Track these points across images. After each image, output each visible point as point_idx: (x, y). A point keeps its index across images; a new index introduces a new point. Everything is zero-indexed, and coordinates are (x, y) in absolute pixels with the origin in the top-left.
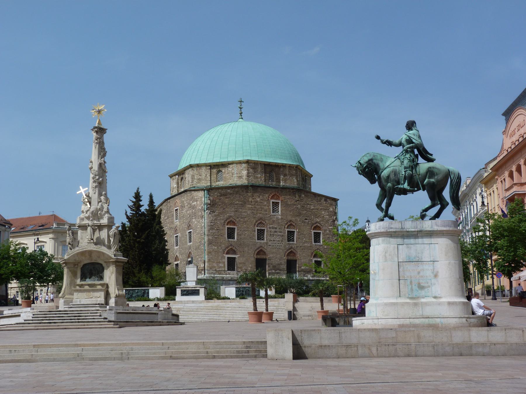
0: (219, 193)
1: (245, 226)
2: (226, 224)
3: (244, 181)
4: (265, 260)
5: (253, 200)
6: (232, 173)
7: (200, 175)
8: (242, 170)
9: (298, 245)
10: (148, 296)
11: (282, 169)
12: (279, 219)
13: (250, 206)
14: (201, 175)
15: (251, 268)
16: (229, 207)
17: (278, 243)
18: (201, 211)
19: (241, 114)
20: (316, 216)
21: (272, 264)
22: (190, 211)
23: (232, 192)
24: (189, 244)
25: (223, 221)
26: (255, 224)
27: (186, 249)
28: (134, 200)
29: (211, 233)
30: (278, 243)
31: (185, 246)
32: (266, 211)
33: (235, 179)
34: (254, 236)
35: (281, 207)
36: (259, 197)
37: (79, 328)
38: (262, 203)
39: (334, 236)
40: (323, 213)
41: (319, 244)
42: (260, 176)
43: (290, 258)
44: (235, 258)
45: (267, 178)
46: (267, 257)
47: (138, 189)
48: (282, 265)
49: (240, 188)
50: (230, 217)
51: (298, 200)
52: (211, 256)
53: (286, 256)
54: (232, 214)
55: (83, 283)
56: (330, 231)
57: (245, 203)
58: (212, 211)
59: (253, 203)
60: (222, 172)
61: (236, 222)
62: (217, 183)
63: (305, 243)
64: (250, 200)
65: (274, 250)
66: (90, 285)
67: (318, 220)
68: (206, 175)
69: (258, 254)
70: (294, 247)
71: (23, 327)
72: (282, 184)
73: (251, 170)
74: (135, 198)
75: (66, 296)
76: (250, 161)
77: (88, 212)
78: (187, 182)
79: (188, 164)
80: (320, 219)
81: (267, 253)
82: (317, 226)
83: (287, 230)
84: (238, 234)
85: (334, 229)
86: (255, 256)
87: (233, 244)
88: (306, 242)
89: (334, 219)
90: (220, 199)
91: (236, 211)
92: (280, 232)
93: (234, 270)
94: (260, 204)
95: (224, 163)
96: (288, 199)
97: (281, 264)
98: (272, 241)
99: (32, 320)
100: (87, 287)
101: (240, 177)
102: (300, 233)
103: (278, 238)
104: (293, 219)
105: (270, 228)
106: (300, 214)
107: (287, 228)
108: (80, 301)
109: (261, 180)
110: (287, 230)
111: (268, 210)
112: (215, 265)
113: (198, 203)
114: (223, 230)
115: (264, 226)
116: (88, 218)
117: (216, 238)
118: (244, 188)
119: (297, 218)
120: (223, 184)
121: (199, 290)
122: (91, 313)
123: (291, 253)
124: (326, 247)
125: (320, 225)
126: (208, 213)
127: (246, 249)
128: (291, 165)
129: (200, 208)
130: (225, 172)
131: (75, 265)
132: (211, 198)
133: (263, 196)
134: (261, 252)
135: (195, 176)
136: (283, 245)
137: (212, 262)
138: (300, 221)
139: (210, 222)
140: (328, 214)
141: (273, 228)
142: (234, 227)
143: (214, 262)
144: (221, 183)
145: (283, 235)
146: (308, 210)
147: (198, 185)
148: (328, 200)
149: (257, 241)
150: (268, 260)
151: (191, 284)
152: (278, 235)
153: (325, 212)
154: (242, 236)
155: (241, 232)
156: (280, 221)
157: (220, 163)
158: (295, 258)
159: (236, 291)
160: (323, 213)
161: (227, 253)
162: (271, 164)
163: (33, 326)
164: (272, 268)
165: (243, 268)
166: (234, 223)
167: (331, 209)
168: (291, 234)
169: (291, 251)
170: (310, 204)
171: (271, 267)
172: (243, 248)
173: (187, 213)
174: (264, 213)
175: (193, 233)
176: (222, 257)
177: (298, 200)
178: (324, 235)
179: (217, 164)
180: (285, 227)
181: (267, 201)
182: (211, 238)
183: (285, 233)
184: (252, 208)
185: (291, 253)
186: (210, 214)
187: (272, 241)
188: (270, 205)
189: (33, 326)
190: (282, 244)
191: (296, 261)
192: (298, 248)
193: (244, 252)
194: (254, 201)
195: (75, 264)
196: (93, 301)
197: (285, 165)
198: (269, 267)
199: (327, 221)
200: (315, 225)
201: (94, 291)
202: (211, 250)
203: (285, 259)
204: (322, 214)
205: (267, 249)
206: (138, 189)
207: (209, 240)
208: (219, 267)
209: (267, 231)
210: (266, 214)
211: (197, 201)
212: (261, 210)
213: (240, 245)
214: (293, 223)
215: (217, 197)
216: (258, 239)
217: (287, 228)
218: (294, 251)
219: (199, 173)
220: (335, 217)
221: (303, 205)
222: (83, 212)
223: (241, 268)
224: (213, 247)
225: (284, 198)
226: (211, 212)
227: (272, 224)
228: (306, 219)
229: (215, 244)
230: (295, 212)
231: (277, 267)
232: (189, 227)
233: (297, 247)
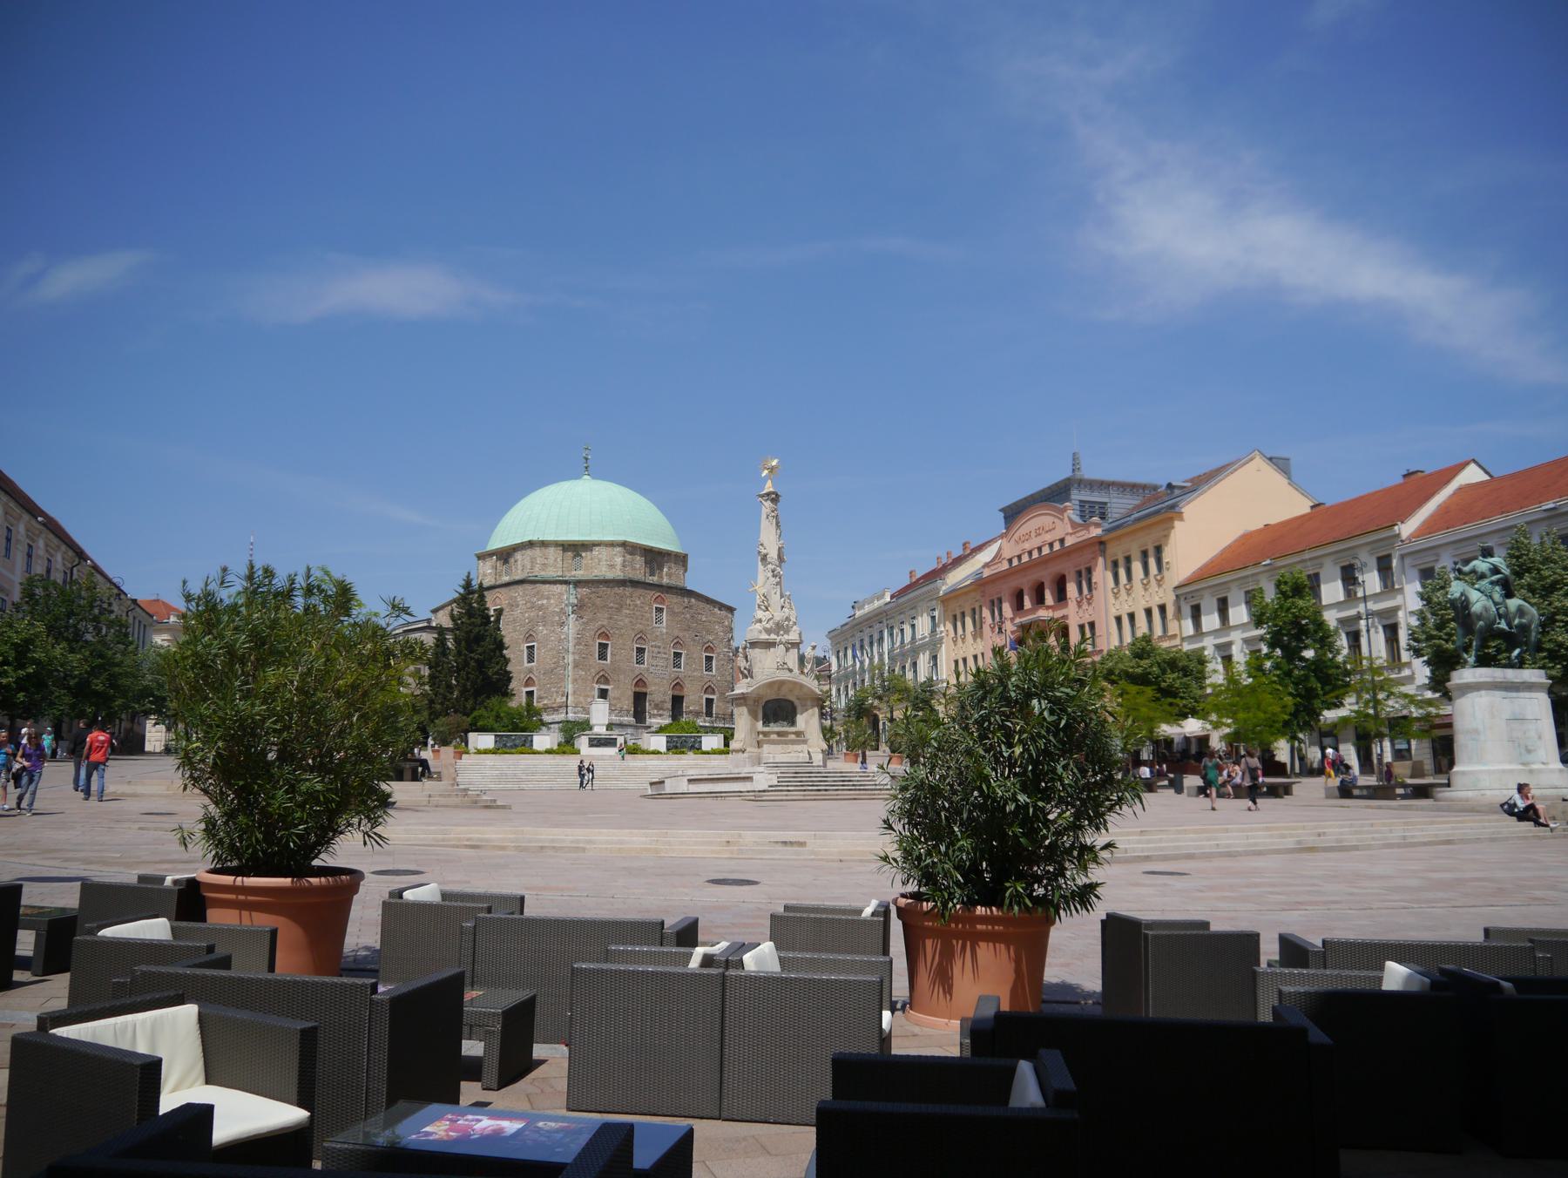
3: (617, 574)
4: (645, 694)
8: (615, 555)
10: (532, 745)
11: (666, 558)
13: (628, 612)
16: (600, 611)
18: (559, 616)
19: (586, 468)
20: (709, 632)
22: (532, 614)
24: (526, 665)
25: (593, 633)
27: (520, 672)
28: (462, 591)
31: (518, 668)
33: (604, 569)
34: (632, 657)
37: (855, 799)
38: (642, 607)
40: (717, 627)
41: (711, 673)
43: (677, 693)
47: (469, 573)
50: (603, 626)
54: (605, 623)
55: (766, 729)
57: (622, 607)
59: (632, 608)
60: (581, 556)
62: (573, 573)
63: (694, 671)
64: (628, 602)
66: (779, 734)
68: (556, 559)
71: (787, 795)
72: (665, 581)
74: (463, 588)
75: (748, 750)
77: (771, 622)
78: (520, 567)
79: (526, 539)
83: (673, 651)
86: (633, 688)
87: (606, 668)
88: (695, 670)
92: (665, 653)
99: (776, 786)
100: (774, 737)
101: (612, 566)
104: (681, 635)
105: (652, 646)
106: (689, 628)
108: (774, 757)
110: (673, 651)
112: (582, 699)
113: (552, 601)
114: (592, 646)
116: (768, 631)
117: (584, 658)
118: (622, 583)
120: (582, 575)
121: (616, 739)
122: (860, 776)
123: (678, 686)
127: (622, 677)
129: (556, 609)
130: (586, 557)
131: (755, 702)
132: (579, 596)
134: (640, 682)
135: (538, 559)
143: (580, 695)
144: (580, 574)
147: (543, 573)
151: (600, 730)
154: (617, 658)
156: (665, 637)
159: (667, 742)
161: (597, 683)
163: (801, 795)
168: (678, 655)
171: (653, 706)
173: (524, 616)
174: (646, 623)
175: (538, 649)
178: (717, 661)
182: (577, 657)
185: (678, 686)
186: (577, 620)
189: (801, 795)
191: (683, 697)
195: (756, 701)
196: (792, 757)
198: (650, 705)
201: (786, 743)
204: (715, 629)
205: (649, 679)
206: (469, 573)
209: (648, 652)
211: (548, 598)
216: (637, 663)
217: (673, 648)
222: (760, 621)
223: (615, 705)
232: (529, 637)
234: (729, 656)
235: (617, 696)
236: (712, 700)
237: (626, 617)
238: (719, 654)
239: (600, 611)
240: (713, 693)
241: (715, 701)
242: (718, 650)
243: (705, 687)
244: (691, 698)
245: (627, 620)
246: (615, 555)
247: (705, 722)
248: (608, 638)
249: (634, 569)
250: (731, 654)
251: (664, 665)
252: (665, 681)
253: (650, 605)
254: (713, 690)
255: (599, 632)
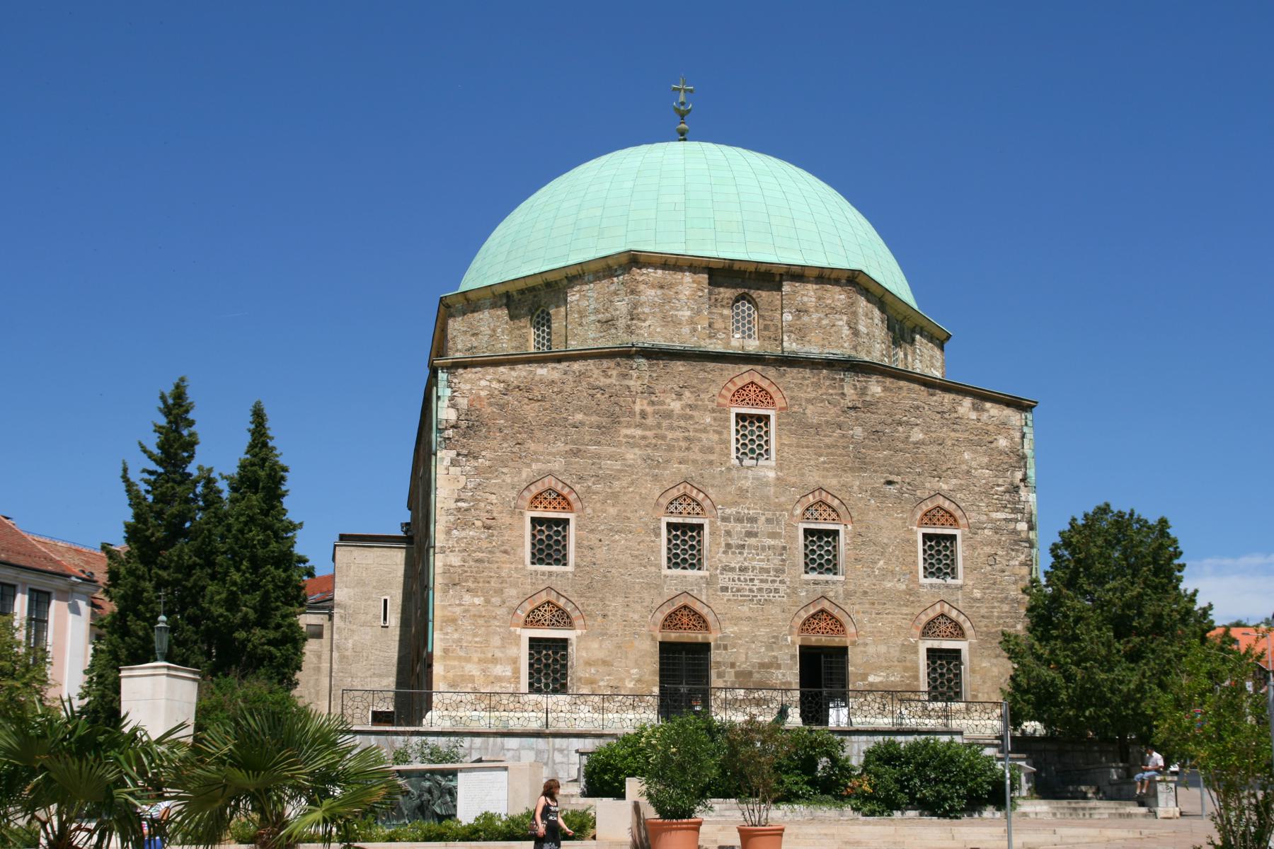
0: (500, 382)
1: (612, 511)
2: (526, 504)
4: (705, 647)
5: (649, 409)
6: (579, 312)
7: (473, 335)
8: (615, 293)
9: (851, 587)
11: (787, 287)
12: (767, 484)
13: (639, 432)
14: (476, 334)
15: (639, 681)
16: (538, 434)
17: (762, 581)
21: (733, 665)
23: (556, 375)
26: (657, 504)
29: (459, 540)
30: (762, 581)
32: (711, 450)
33: (591, 335)
34: (655, 551)
35: (779, 436)
36: (679, 395)
38: (691, 417)
39: (1017, 551)
40: (966, 456)
42: (688, 313)
43: (815, 639)
44: (563, 643)
45: (719, 324)
46: (712, 638)
48: (779, 667)
49: (591, 362)
50: (550, 474)
51: (854, 408)
52: (456, 636)
53: (796, 631)
54: (557, 465)
56: (997, 530)
57: (615, 421)
58: (465, 452)
61: (572, 497)
64: (637, 408)
65: (745, 609)
67: (945, 487)
68: (494, 331)
69: (671, 621)
70: (836, 597)
73: (652, 292)
76: (642, 259)
80: (954, 481)
81: (710, 619)
82: (939, 508)
84: (579, 546)
85: (1016, 521)
88: (887, 574)
89: (1017, 481)
90: (502, 407)
91: (576, 453)
92: (773, 535)
93: (561, 688)
94: (682, 423)
95: (550, 278)
96: (809, 401)
97: (774, 664)
98: (733, 570)
102: (860, 539)
103: (763, 560)
104: (832, 482)
105: (725, 519)
106: (862, 464)
107: (804, 518)
109: (695, 330)
110: (802, 526)
111: (717, 449)
115: (698, 509)
119: (848, 478)
124: (977, 594)
125: (953, 506)
126: (447, 462)
128: (827, 273)
130: (557, 313)
133: (697, 392)
136: (782, 588)
137: (460, 658)
138: (861, 490)
139: (456, 496)
140: (986, 460)
141: (739, 520)
142: (563, 516)
143: (468, 660)
145: (784, 548)
146: (902, 446)
148: (988, 405)
149: (669, 572)
150: (718, 647)
152: (763, 548)
153: (975, 452)
154: (601, 554)
155: (591, 536)
157: (539, 280)
158: (836, 641)
160: (966, 456)
161: (532, 620)
162: (736, 267)
164: (733, 683)
165: (601, 683)
166: (564, 498)
167: (1003, 443)
169: (822, 611)
170: (907, 423)
171: (730, 676)
172: (602, 600)
174: (699, 457)
176: (503, 639)
177: (854, 408)
179: (531, 283)
180: (792, 515)
181: (713, 411)
182: (455, 560)
183: (794, 538)
184: (644, 438)
186: (454, 463)
187: (733, 570)
188: (728, 428)
190: (782, 582)
191: (842, 651)
192: (854, 599)
193: (604, 616)
194: (655, 413)
197: (799, 270)
199: (986, 492)
200: (930, 506)
202: (458, 610)
203: (793, 643)
204: (963, 462)
207: (448, 569)
208: (492, 679)
210: (711, 463)
212: (688, 449)
213: (589, 587)
214: (829, 500)
215: (491, 396)
217: (804, 518)
218: (836, 612)
219: (471, 326)
220: (1019, 475)
221: (879, 428)
223: (591, 682)
224: (467, 598)
225: (792, 398)
226: (458, 455)
227: (735, 504)
228: (890, 483)
229: (470, 584)
230: (841, 455)
231: (756, 676)
233: (848, 595)
234: (1015, 532)
235: (600, 655)
236: (958, 651)
237: (632, 444)
238: (975, 529)
239: (538, 434)
240: (958, 631)
241: (965, 656)
242: (974, 517)
243: (924, 619)
244: (871, 650)
245: (632, 455)
246: (615, 293)
247: (926, 713)
248: (568, 506)
249: (669, 321)
250: (1023, 526)
251: (776, 561)
252: (778, 610)
253: (721, 409)
254: (957, 626)
255: (535, 490)
